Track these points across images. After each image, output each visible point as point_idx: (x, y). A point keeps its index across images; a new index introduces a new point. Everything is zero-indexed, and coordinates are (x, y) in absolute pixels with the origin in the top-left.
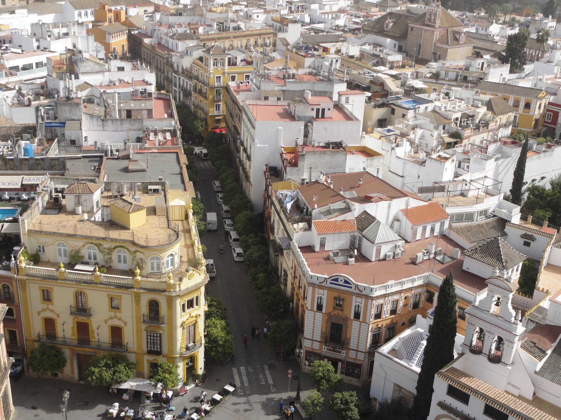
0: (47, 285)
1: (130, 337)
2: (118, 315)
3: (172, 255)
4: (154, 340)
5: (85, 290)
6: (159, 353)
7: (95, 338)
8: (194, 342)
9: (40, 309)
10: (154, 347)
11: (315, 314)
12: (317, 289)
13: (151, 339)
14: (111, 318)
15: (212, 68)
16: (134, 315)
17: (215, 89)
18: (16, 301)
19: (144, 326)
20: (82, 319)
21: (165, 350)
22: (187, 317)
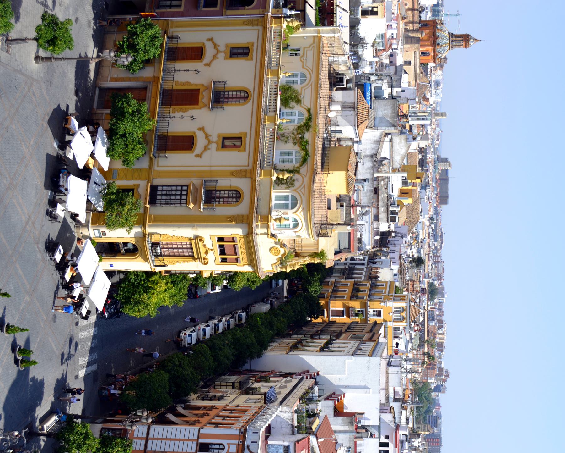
0: (255, 52)
1: (175, 161)
2: (214, 146)
3: (296, 225)
4: (175, 195)
5: (251, 101)
6: (153, 201)
7: (174, 112)
8: (161, 255)
9: (216, 41)
10: (162, 195)
11: (193, 440)
12: (237, 442)
13: (176, 190)
14: (207, 136)
15: (392, 305)
16: (213, 168)
17: (364, 310)
18: (229, 12)
19: (195, 181)
20: (206, 97)
21: (161, 210)
22: (209, 246)
